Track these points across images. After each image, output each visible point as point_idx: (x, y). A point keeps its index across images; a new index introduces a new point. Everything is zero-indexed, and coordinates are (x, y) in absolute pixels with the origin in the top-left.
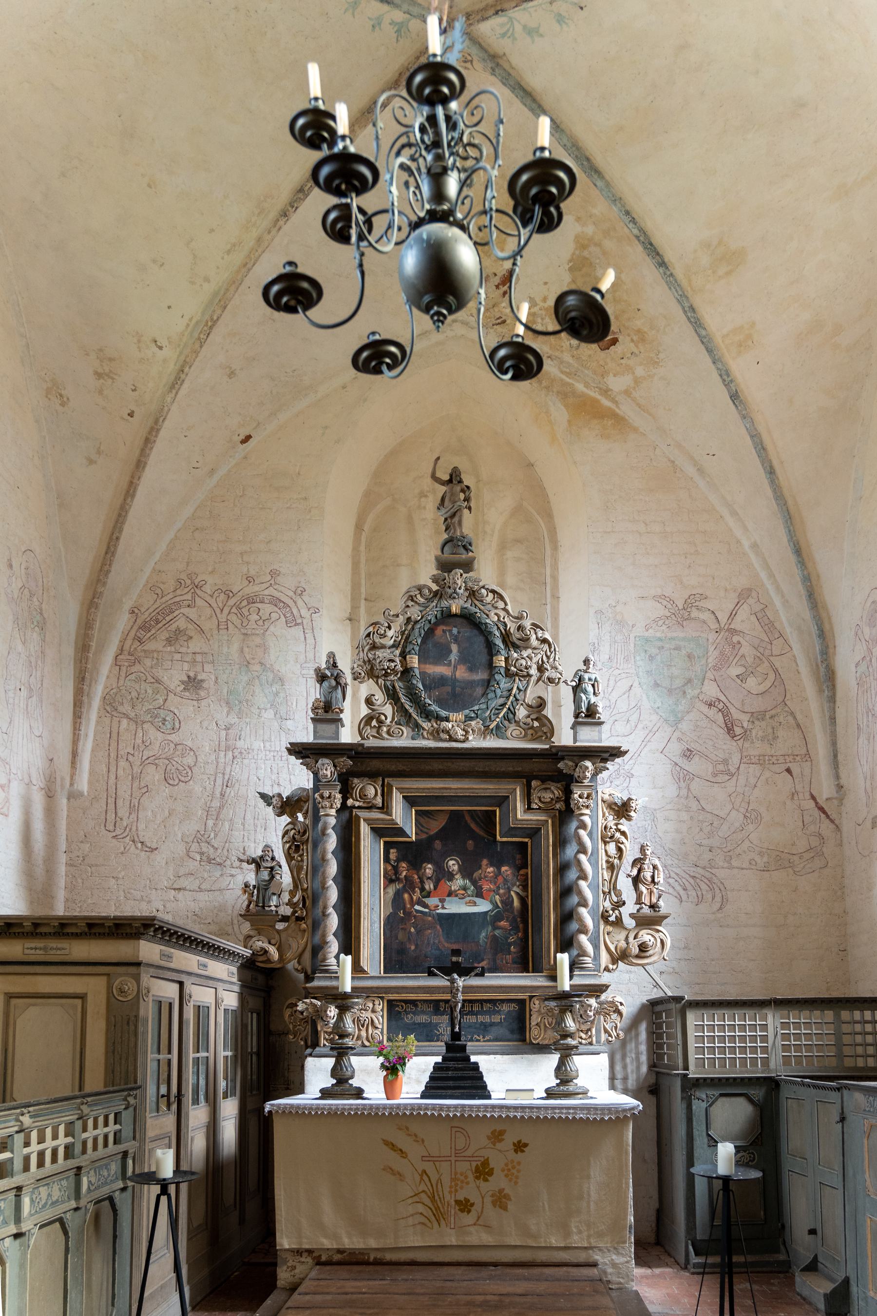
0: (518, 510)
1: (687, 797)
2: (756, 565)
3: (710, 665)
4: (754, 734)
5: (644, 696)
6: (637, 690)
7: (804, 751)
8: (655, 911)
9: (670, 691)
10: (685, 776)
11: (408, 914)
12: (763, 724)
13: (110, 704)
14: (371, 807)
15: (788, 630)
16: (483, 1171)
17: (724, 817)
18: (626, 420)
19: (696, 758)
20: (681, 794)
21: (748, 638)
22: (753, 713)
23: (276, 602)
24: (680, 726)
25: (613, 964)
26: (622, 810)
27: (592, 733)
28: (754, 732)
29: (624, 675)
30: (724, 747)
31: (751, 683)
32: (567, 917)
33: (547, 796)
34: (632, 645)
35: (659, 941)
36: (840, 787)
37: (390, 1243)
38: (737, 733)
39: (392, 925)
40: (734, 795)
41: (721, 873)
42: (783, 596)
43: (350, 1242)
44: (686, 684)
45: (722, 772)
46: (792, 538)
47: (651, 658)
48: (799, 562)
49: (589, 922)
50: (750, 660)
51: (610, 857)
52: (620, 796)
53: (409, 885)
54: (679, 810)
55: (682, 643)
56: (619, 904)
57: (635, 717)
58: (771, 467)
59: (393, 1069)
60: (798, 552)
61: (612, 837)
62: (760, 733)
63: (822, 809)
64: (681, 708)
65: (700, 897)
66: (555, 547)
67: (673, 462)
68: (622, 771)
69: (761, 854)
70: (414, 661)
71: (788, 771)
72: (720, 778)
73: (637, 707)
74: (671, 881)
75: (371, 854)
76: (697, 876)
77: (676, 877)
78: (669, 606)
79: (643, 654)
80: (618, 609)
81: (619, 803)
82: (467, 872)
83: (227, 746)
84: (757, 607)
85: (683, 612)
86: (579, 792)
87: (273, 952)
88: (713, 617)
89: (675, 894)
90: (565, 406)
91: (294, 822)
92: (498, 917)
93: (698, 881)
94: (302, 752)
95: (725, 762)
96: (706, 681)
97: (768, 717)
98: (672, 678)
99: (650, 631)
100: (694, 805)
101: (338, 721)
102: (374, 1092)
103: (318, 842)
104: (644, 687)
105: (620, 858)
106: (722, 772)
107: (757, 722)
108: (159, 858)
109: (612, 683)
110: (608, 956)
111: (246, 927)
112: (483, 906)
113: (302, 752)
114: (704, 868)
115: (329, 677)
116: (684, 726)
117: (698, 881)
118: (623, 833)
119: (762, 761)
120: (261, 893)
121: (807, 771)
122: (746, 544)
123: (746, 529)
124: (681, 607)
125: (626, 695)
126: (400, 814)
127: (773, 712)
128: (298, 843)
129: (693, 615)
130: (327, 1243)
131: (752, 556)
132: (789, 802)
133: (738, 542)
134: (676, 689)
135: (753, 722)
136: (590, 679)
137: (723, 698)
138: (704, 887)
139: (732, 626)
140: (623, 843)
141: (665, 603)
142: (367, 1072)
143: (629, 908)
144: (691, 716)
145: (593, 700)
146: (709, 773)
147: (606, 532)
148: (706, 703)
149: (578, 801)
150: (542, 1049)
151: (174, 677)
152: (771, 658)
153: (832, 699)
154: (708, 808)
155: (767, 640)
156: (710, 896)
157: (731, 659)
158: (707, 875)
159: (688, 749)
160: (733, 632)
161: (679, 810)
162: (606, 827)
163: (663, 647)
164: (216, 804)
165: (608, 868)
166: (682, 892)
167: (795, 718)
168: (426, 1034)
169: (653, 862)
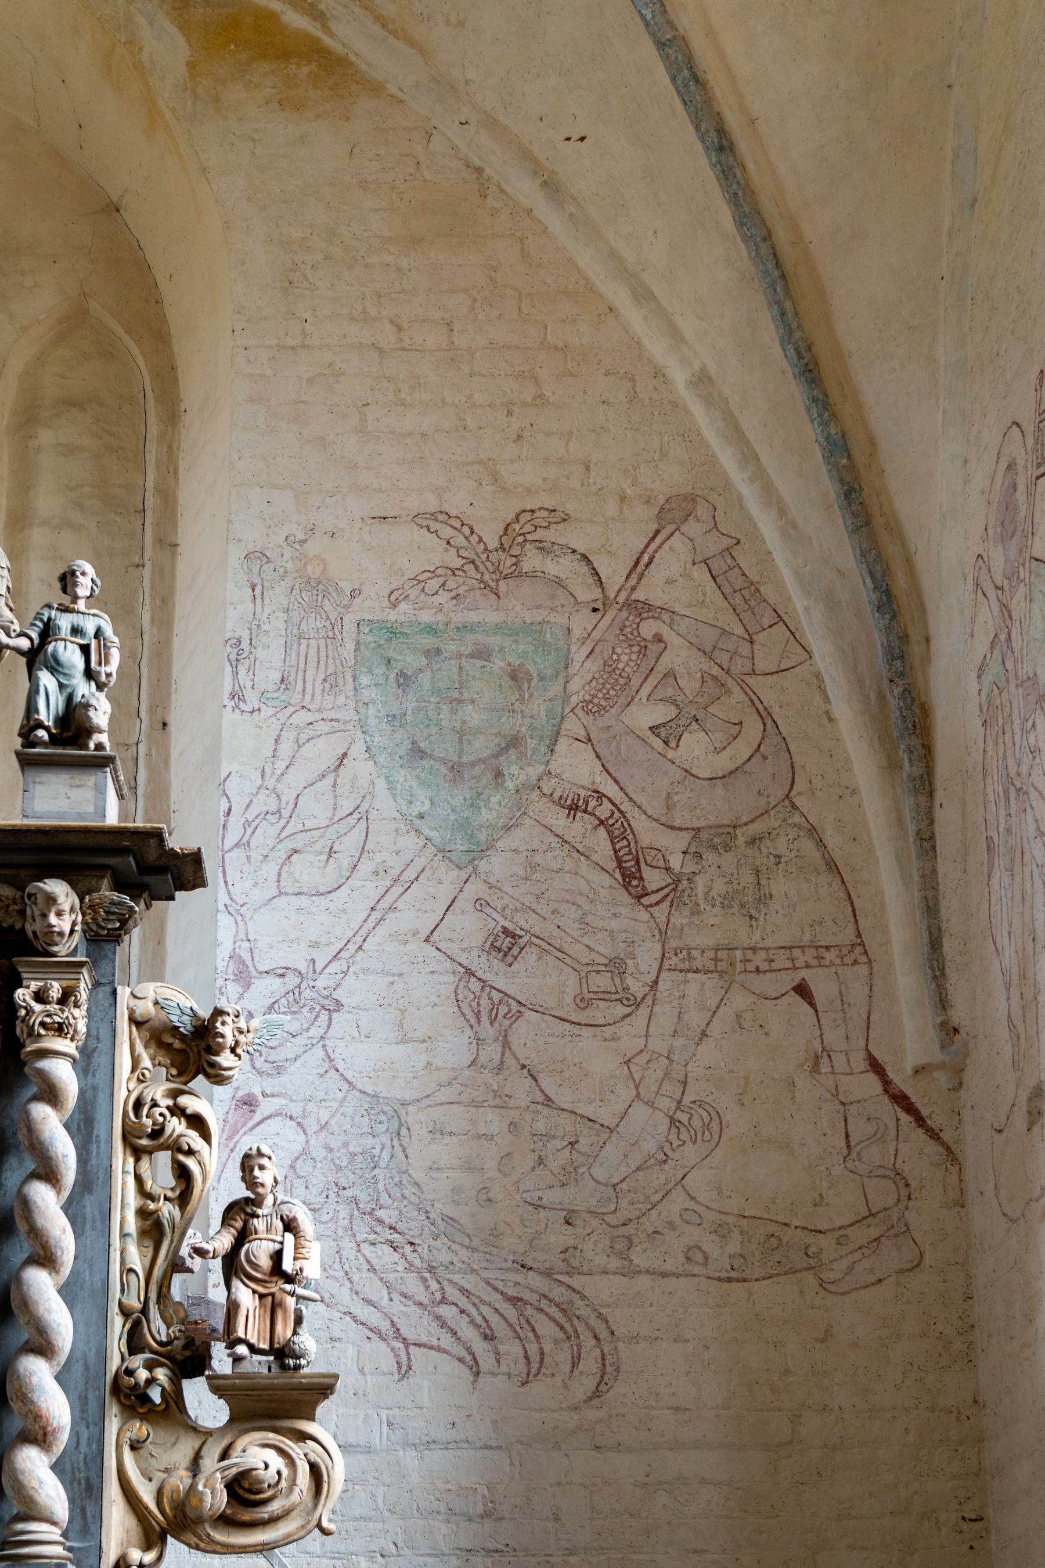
0: (75, 321)
1: (500, 1068)
2: (710, 435)
3: (574, 700)
4: (700, 889)
5: (381, 785)
6: (360, 767)
7: (847, 935)
8: (284, 1367)
9: (457, 770)
10: (494, 1006)
12: (728, 860)
15: (799, 603)
17: (611, 1122)
18: (351, 64)
19: (530, 957)
20: (483, 1059)
21: (683, 625)
22: (698, 830)
24: (483, 866)
25: (147, 1548)
26: (192, 1049)
27: (76, 794)
28: (700, 884)
29: (323, 727)
30: (614, 924)
31: (694, 748)
34: (350, 646)
35: (303, 1468)
36: (950, 1031)
38: (652, 886)
40: (642, 1059)
41: (600, 1289)
42: (782, 512)
44: (503, 751)
45: (605, 996)
46: (790, 333)
47: (404, 680)
48: (815, 400)
50: (689, 685)
51: (152, 1197)
52: (181, 1000)
54: (474, 1104)
55: (495, 641)
57: (350, 843)
58: (722, 132)
60: (810, 370)
61: (157, 1133)
62: (720, 887)
63: (901, 1100)
64: (486, 815)
65: (535, 1358)
67: (479, 170)
68: (308, 994)
69: (721, 1231)
71: (802, 990)
72: (600, 1012)
73: (361, 814)
74: (447, 1312)
76: (527, 1295)
77: (463, 1301)
78: (460, 541)
79: (380, 670)
80: (313, 548)
81: (185, 1025)
84: (713, 545)
85: (500, 557)
86: (34, 985)
88: (584, 569)
89: (459, 1351)
90: (181, 28)
93: (529, 1311)
95: (616, 966)
96: (562, 745)
97: (741, 840)
98: (462, 733)
99: (403, 606)
100: (521, 1090)
104: (382, 759)
105: (184, 1198)
106: (605, 996)
107: (710, 857)
109: (286, 747)
110: (132, 1522)
114: (548, 1273)
116: (496, 866)
117: (529, 1311)
118: (197, 1122)
119: (726, 964)
121: (857, 992)
122: (679, 376)
123: (678, 338)
124: (492, 543)
125: (329, 781)
127: (758, 827)
129: (526, 567)
131: (698, 410)
132: (803, 1081)
133: (658, 373)
134: (473, 764)
135: (699, 856)
136: (76, 631)
137: (610, 789)
138: (546, 1328)
139: (639, 595)
140: (190, 1152)
141: (447, 532)
144: (516, 839)
145: (83, 689)
146: (568, 999)
147: (282, 347)
148: (561, 803)
149: (30, 1011)
152: (751, 680)
153: (924, 785)
154: (563, 1097)
155: (740, 631)
156: (564, 1357)
157: (635, 682)
158: (558, 1293)
159: (505, 931)
160: (642, 609)
161: (474, 1104)
162: (138, 1105)
163: (438, 651)
165: (143, 1233)
166: (480, 1347)
167: (820, 843)
169: (285, 1210)
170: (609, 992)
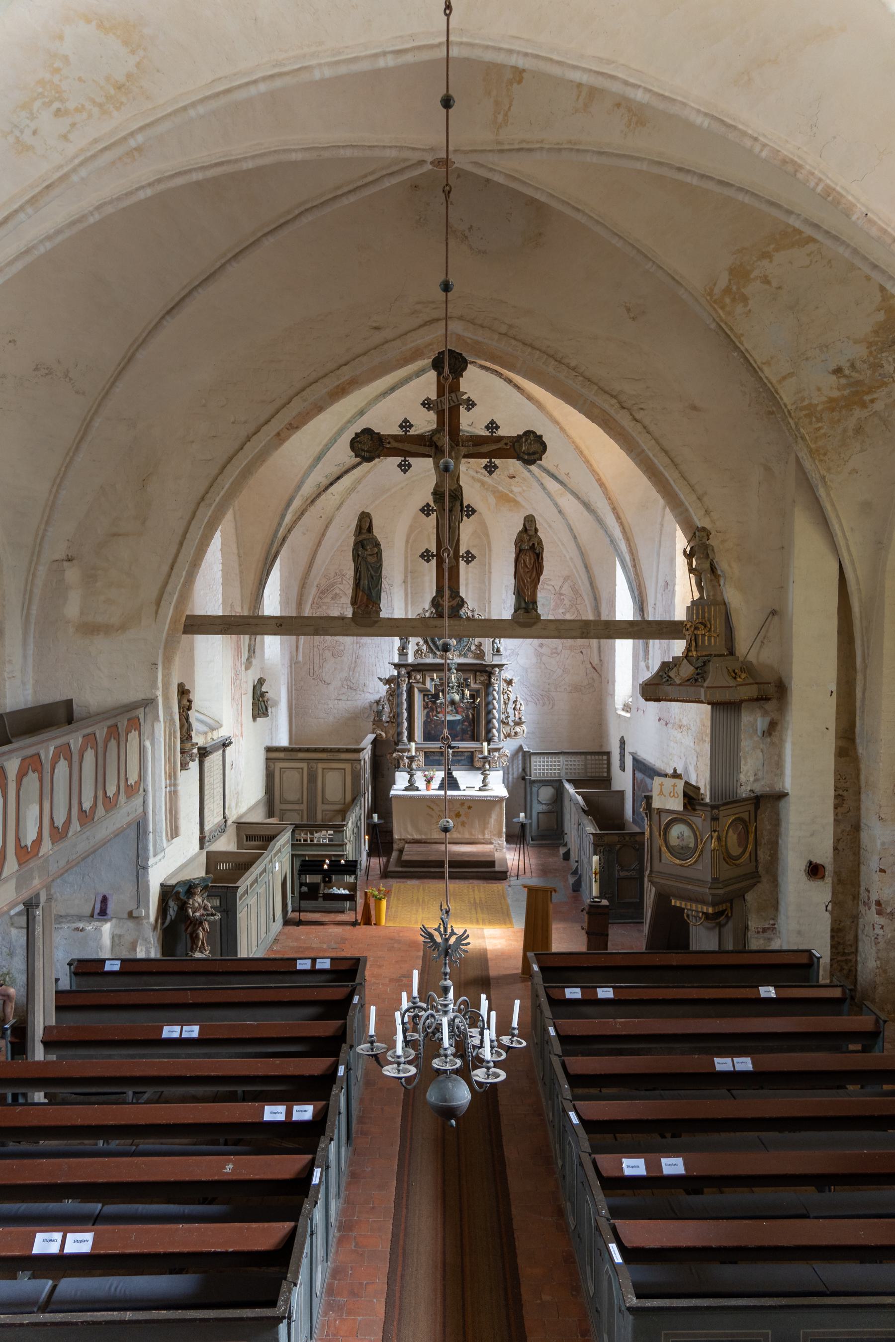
11: (431, 720)
14: (418, 682)
16: (458, 815)
26: (509, 683)
32: (489, 722)
33: (482, 679)
36: (601, 660)
37: (429, 837)
39: (426, 724)
43: (417, 836)
49: (497, 725)
52: (509, 677)
53: (432, 710)
56: (508, 717)
66: (490, 550)
87: (384, 734)
91: (390, 687)
92: (464, 721)
95: (556, 648)
100: (543, 666)
101: (406, 654)
108: (331, 688)
112: (459, 717)
130: (409, 837)
142: (420, 782)
160: (561, 594)
164: (353, 666)
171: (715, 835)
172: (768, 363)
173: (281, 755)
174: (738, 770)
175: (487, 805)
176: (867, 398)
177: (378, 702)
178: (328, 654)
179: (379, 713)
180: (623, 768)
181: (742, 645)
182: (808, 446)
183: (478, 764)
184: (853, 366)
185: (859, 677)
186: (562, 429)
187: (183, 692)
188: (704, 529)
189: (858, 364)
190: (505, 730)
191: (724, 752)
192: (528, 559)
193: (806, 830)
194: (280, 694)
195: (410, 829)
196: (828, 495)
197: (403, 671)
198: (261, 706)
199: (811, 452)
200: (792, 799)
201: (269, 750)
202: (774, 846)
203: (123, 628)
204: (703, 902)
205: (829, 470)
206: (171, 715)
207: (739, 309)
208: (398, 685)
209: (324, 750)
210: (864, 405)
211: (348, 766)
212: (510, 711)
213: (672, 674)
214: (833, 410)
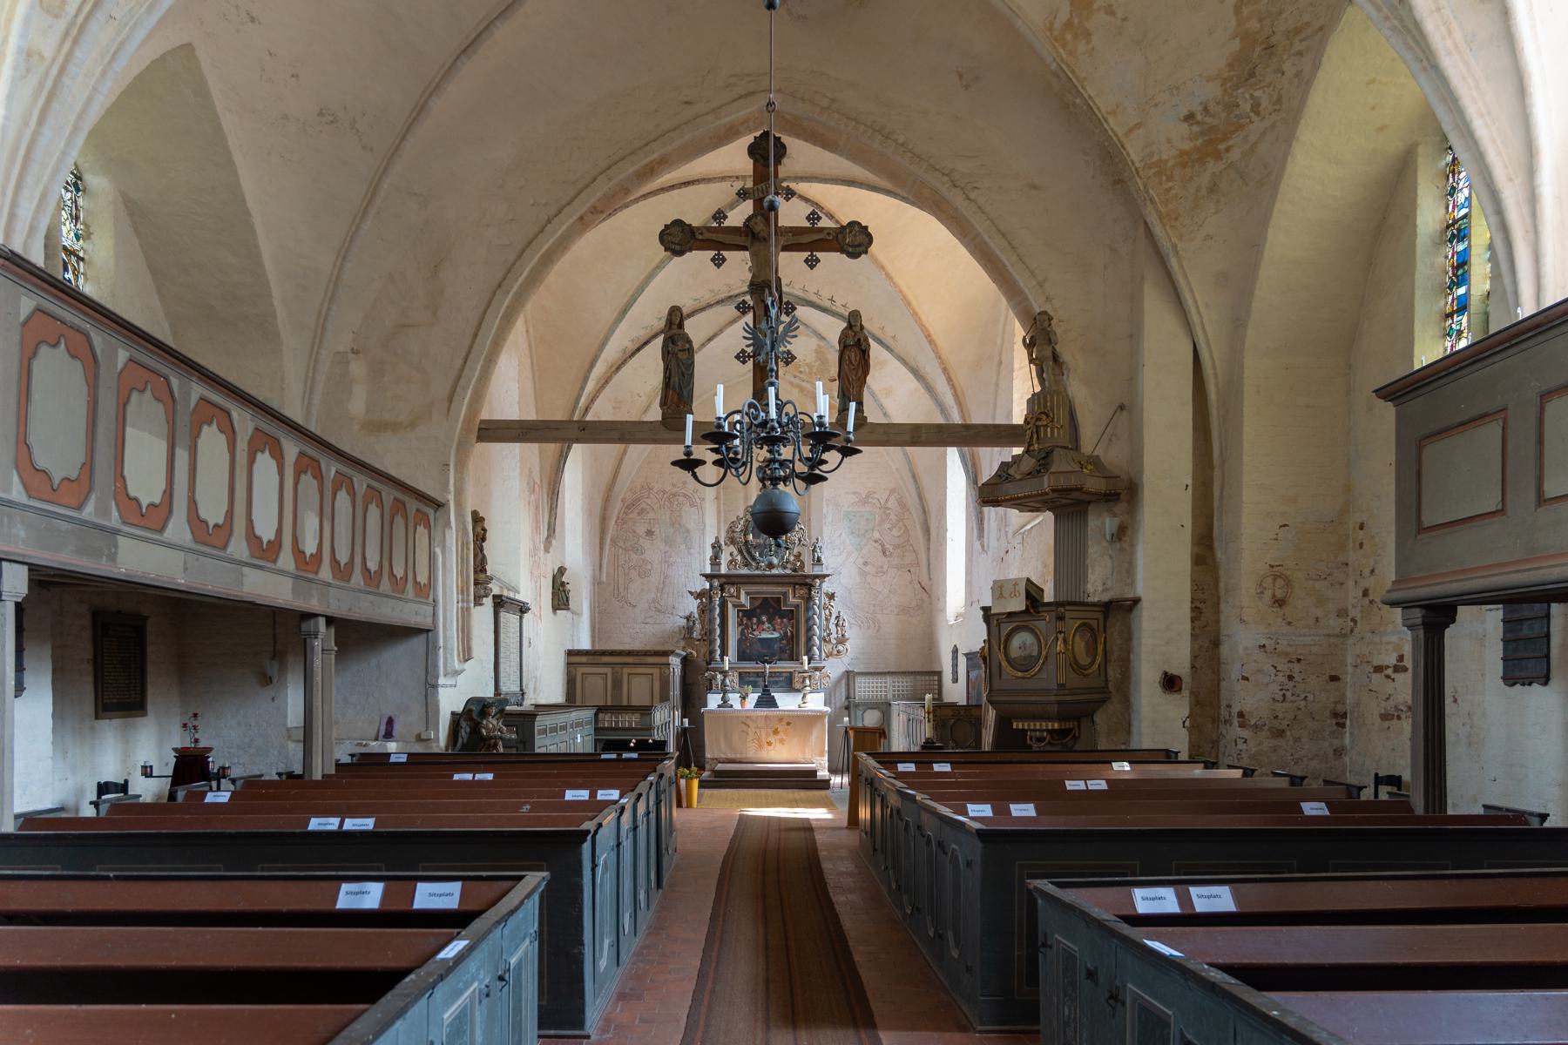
13: (614, 542)
23: (685, 495)
26: (831, 597)
31: (895, 532)
32: (809, 639)
39: (740, 642)
43: (730, 756)
52: (831, 591)
53: (747, 627)
59: (743, 698)
70: (751, 537)
75: (732, 614)
82: (770, 621)
83: (666, 561)
94: (707, 576)
102: (737, 706)
103: (712, 610)
108: (637, 610)
111: (682, 643)
112: (776, 635)
113: (707, 576)
115: (716, 547)
119: (899, 567)
120: (690, 630)
126: (744, 599)
128: (703, 610)
142: (734, 699)
143: (834, 635)
150: (798, 691)
151: (641, 530)
168: (755, 685)
170: (881, 571)
171: (1061, 637)
172: (1113, 112)
173: (584, 659)
174: (1085, 580)
175: (811, 719)
176: (1222, 147)
177: (688, 618)
178: (634, 574)
179: (690, 630)
180: (955, 680)
181: (1088, 445)
182: (1157, 210)
183: (797, 686)
184: (1206, 110)
185: (1217, 473)
186: (888, 276)
187: (478, 519)
188: (1044, 313)
189: (1212, 106)
190: (827, 648)
191: (1069, 557)
192: (853, 355)
193: (1162, 637)
194: (582, 597)
195: (723, 746)
196: (1181, 266)
197: (716, 583)
198: (560, 598)
199: (1160, 217)
200: (1144, 604)
201: (570, 653)
202: (1126, 664)
203: (412, 425)
204: (1049, 718)
205: (1181, 237)
206: (464, 523)
207: (1082, 47)
208: (711, 599)
209: (630, 653)
210: (1218, 156)
211: (656, 671)
212: (832, 627)
213: (1011, 471)
214: (1184, 165)
